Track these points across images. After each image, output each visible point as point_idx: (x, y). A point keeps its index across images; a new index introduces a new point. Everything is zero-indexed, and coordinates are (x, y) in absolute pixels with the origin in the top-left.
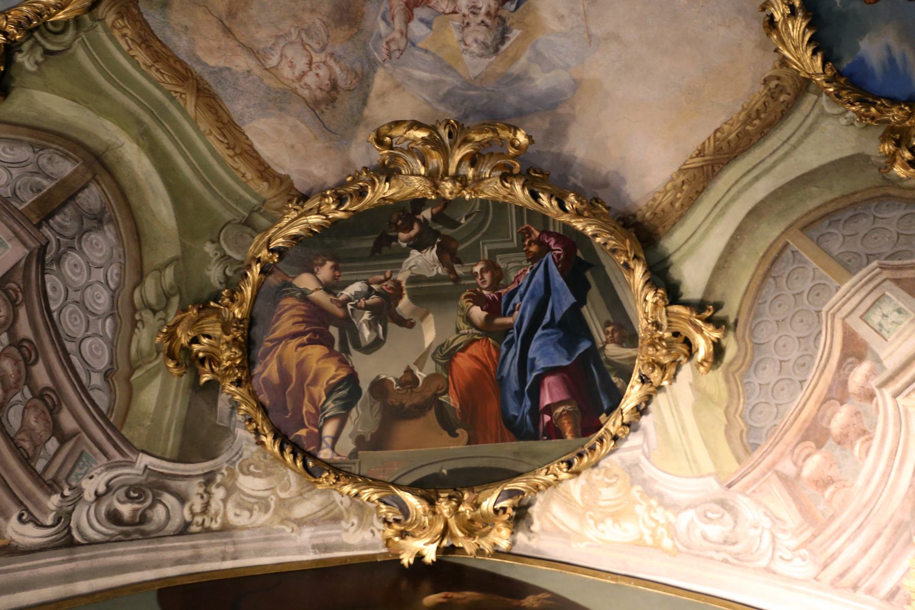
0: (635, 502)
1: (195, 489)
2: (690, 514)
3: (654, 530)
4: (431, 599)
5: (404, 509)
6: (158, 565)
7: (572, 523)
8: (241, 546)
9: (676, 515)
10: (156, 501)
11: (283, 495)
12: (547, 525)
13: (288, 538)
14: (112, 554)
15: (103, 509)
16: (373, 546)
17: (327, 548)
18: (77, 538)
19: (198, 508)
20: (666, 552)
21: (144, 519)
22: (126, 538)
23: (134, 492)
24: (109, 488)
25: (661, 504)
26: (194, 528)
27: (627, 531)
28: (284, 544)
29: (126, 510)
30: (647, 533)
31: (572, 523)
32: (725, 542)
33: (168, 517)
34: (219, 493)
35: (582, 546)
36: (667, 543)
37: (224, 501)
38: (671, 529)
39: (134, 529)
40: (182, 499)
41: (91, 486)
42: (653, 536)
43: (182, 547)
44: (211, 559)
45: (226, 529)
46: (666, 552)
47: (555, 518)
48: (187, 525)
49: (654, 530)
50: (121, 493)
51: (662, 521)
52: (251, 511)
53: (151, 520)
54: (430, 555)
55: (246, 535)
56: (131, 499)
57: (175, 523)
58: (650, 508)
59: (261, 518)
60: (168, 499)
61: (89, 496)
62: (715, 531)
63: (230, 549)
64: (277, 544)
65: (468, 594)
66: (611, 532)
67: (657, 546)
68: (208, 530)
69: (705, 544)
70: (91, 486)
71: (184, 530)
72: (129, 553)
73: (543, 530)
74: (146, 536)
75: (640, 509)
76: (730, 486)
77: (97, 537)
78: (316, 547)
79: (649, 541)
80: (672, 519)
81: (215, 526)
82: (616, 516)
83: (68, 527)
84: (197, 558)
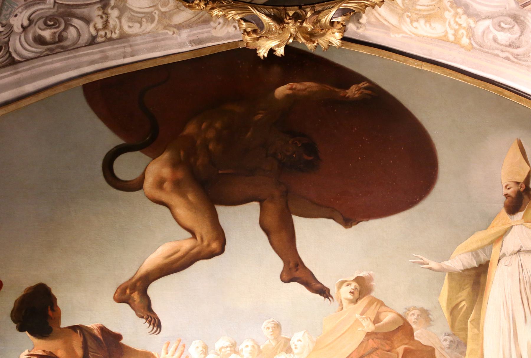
0: (445, 9)
1: (95, 12)
2: (487, 23)
3: (456, 31)
4: (282, 91)
5: (260, 24)
6: (78, 67)
7: (393, 20)
8: (137, 47)
9: (476, 22)
10: (68, 25)
11: (163, 9)
12: (373, 20)
13: (171, 39)
14: (44, 65)
15: (30, 36)
16: (235, 36)
17: (200, 41)
18: (17, 58)
19: (100, 25)
20: (463, 47)
21: (61, 38)
22: (52, 52)
23: (50, 21)
24: (31, 21)
25: (466, 13)
26: (99, 40)
27: (437, 29)
28: (168, 42)
29: (47, 34)
30: (451, 32)
31: (393, 20)
32: (510, 46)
33: (79, 35)
34: (114, 13)
35: (399, 36)
36: (465, 41)
37: (119, 18)
38: (470, 32)
39: (57, 46)
40: (87, 21)
41: (18, 21)
42: (454, 35)
43: (94, 53)
44: (115, 58)
45: (123, 37)
46: (463, 47)
47: (380, 15)
48: (94, 38)
49: (456, 31)
50: (41, 23)
51: (464, 25)
52: (141, 23)
53: (67, 38)
54: (280, 51)
55: (139, 40)
56: (49, 27)
57: (85, 38)
58: (457, 14)
59: (149, 27)
60: (76, 22)
61: (17, 28)
62: (503, 37)
63: (129, 50)
64: (163, 43)
65: (308, 84)
66: (423, 28)
67: (457, 42)
68: (110, 39)
69: (495, 45)
70: (18, 21)
71: (92, 42)
72: (56, 62)
73: (369, 23)
74: (65, 49)
75: (448, 15)
76: (524, 6)
77: (31, 55)
78: (192, 42)
79: (451, 38)
80: (473, 25)
81: (114, 36)
82: (428, 18)
83: (8, 51)
84: (105, 58)
